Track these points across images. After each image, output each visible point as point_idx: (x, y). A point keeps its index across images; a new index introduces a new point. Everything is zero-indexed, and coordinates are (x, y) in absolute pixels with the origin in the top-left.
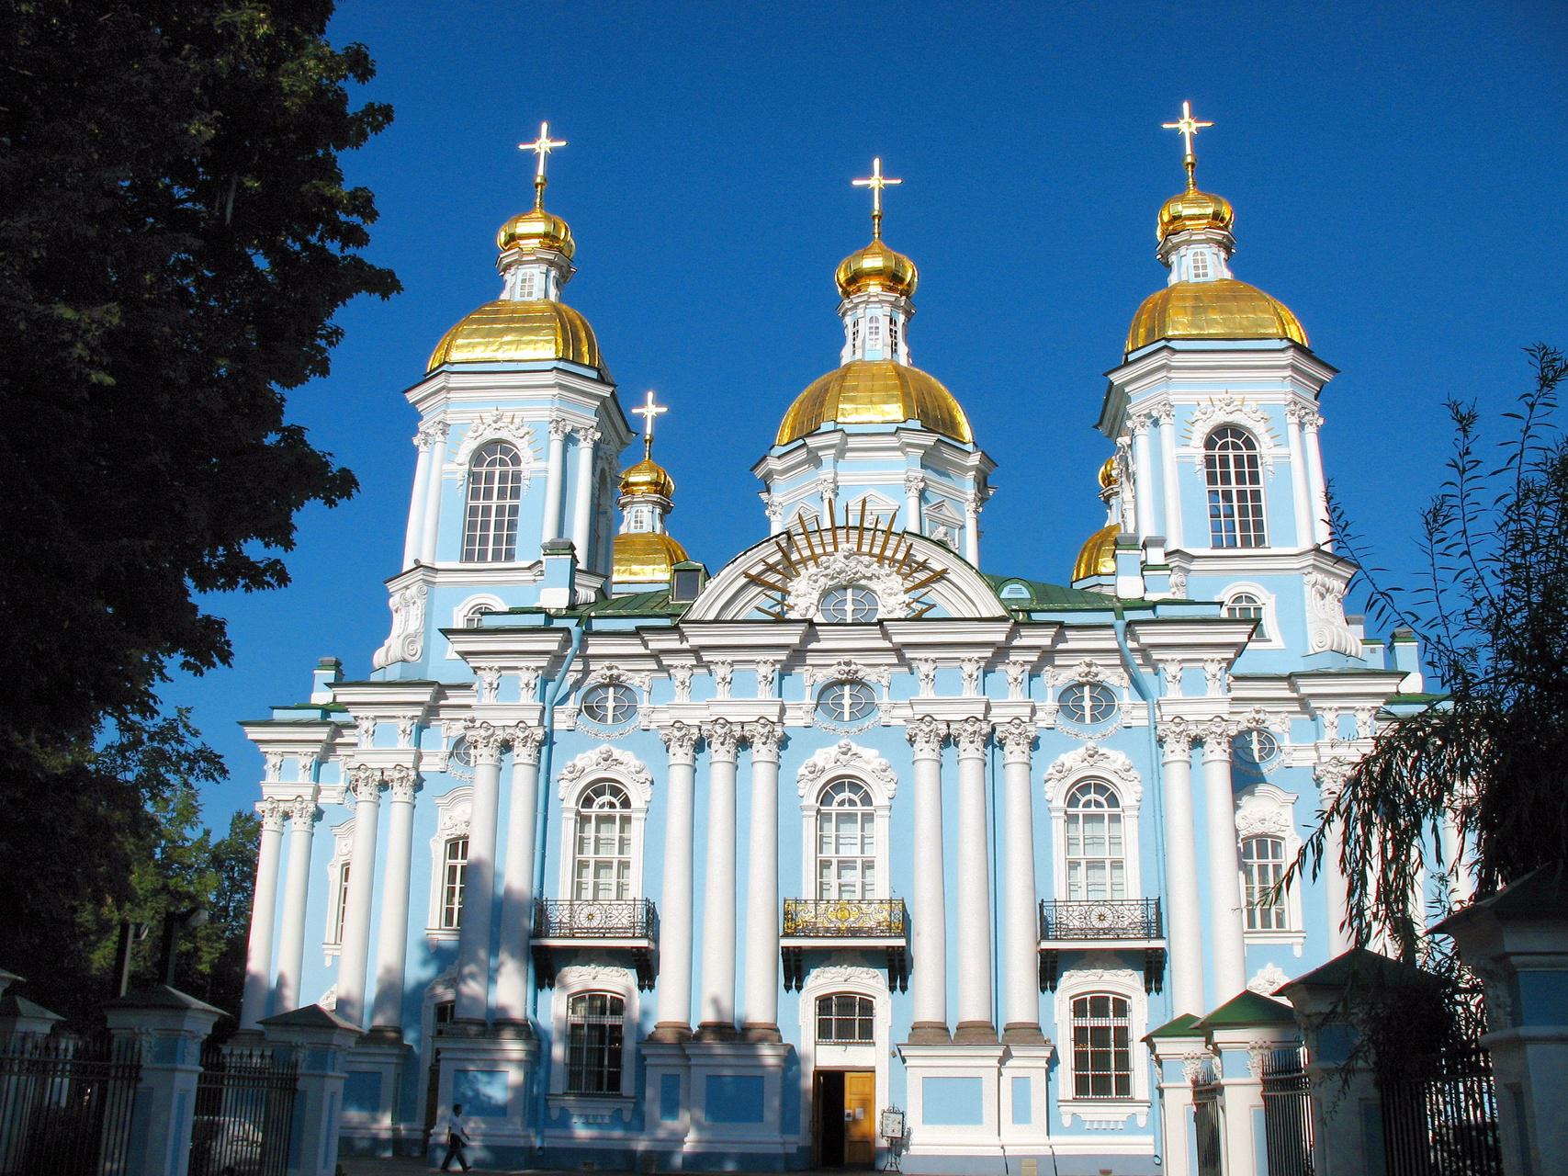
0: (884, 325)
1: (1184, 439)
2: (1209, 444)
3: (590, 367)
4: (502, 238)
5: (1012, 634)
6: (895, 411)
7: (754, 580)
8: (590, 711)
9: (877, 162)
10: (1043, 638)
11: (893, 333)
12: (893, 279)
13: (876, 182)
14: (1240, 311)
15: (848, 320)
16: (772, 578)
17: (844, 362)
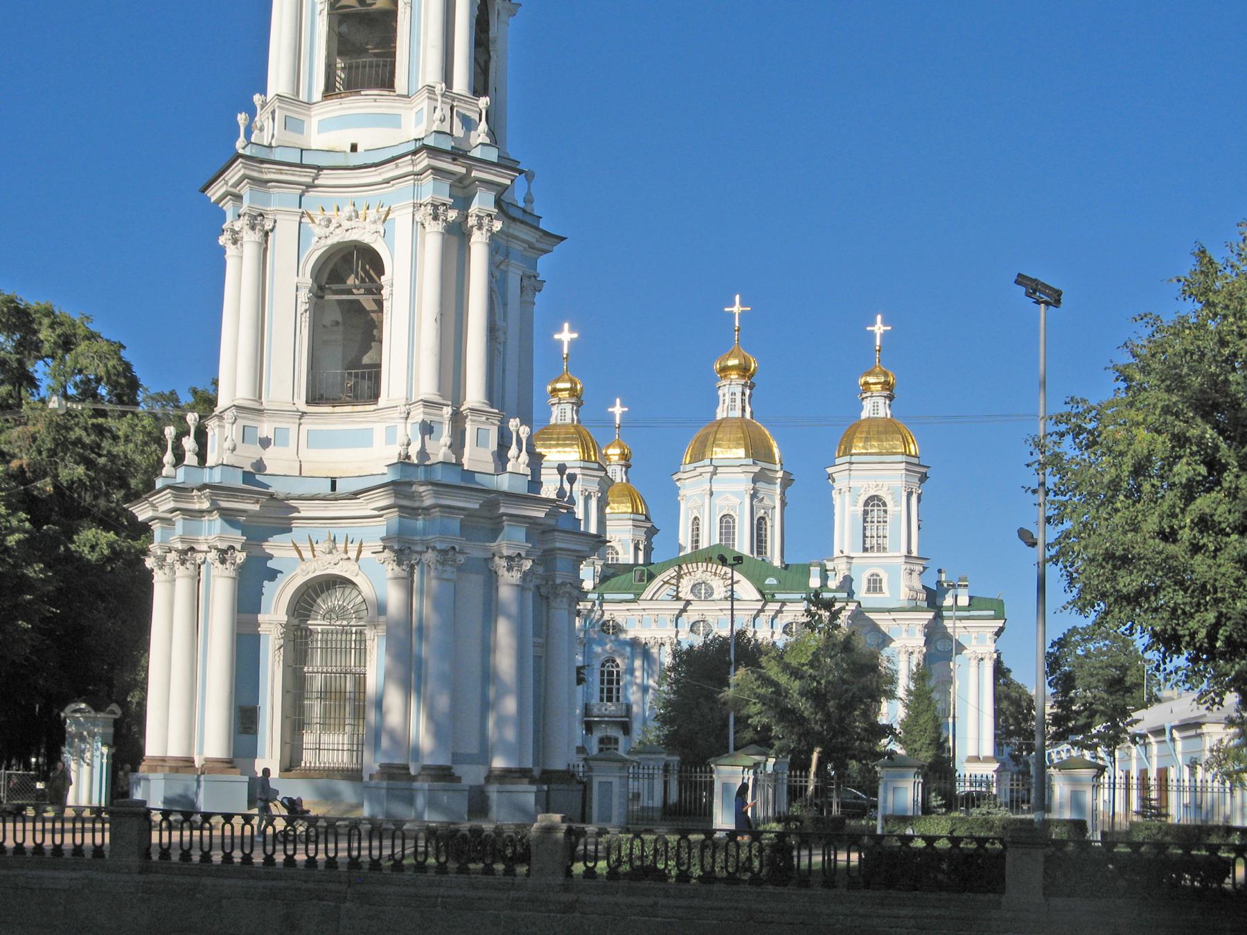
0: (738, 397)
1: (855, 503)
2: (866, 504)
3: (595, 462)
4: (549, 388)
5: (764, 605)
6: (741, 452)
7: (665, 583)
8: (603, 631)
9: (737, 297)
10: (777, 606)
11: (743, 401)
12: (744, 370)
13: (737, 309)
14: (887, 440)
15: (720, 393)
16: (674, 581)
17: (719, 417)
